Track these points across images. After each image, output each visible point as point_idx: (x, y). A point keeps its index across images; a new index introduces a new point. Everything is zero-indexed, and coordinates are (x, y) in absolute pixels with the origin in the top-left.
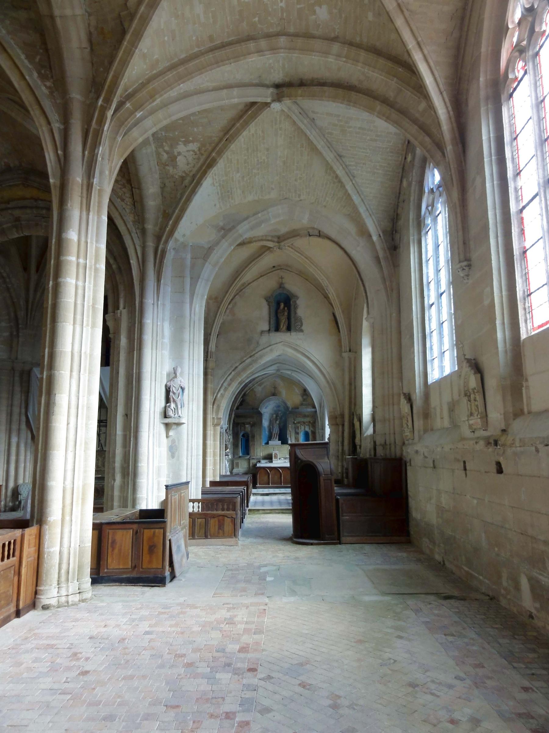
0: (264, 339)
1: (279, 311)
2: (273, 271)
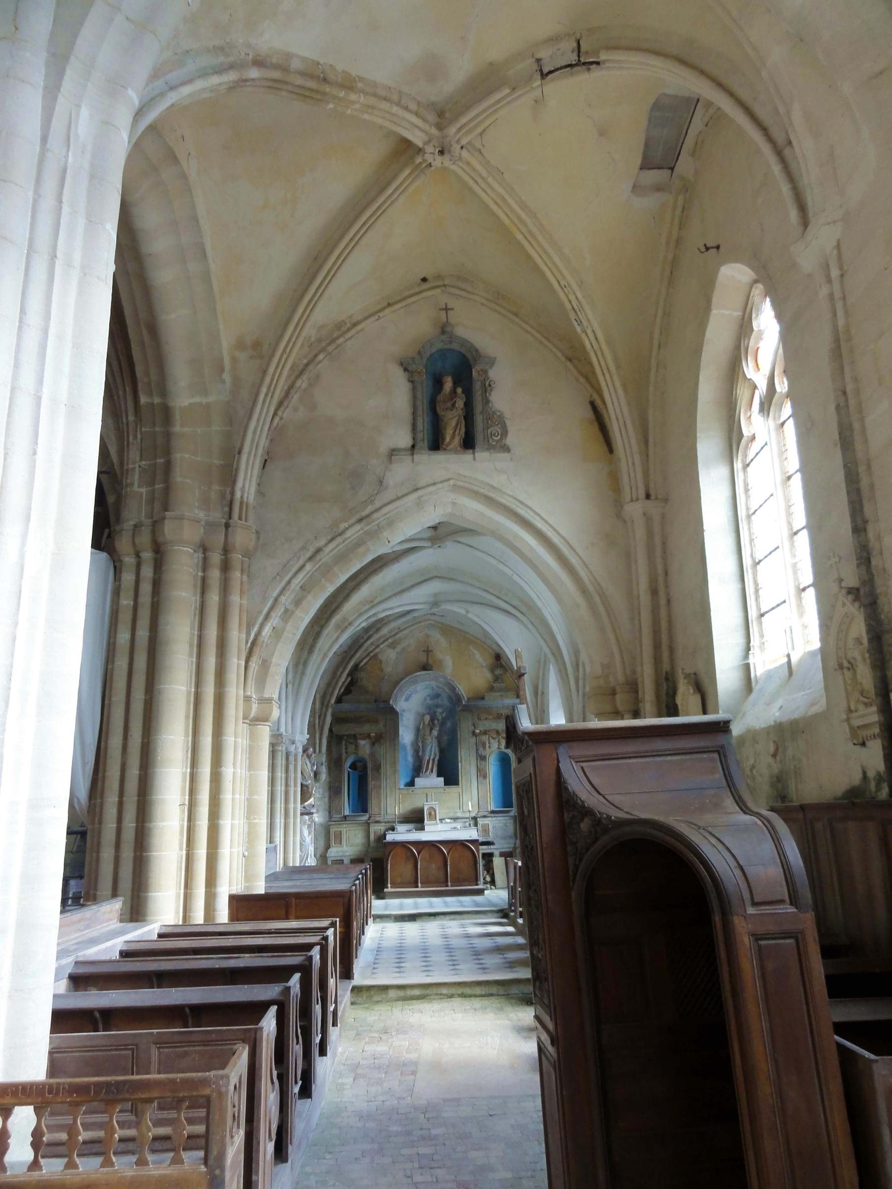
0: (400, 471)
1: (440, 397)
2: (420, 292)
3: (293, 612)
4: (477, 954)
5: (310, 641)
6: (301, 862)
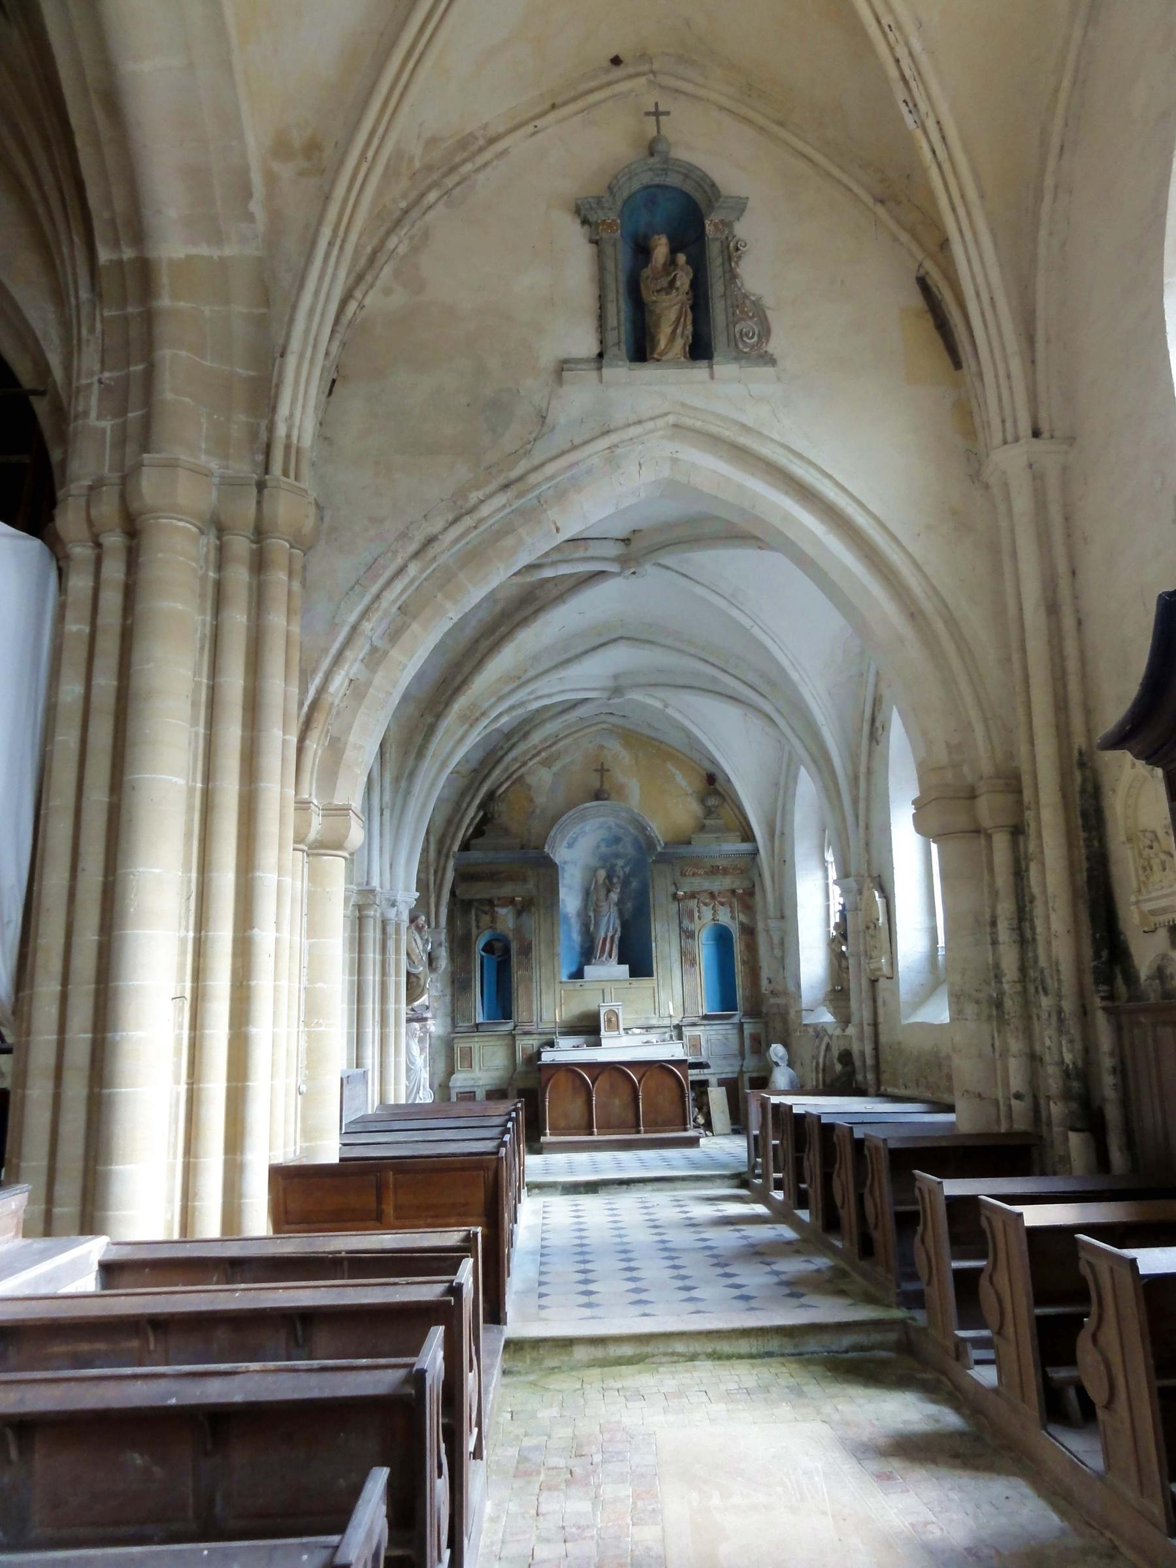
0: (577, 399)
1: (647, 272)
2: (609, 84)
3: (386, 653)
4: (721, 1261)
5: (418, 740)
6: (408, 1098)
